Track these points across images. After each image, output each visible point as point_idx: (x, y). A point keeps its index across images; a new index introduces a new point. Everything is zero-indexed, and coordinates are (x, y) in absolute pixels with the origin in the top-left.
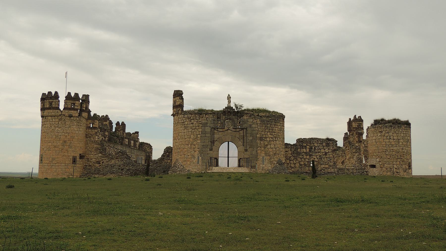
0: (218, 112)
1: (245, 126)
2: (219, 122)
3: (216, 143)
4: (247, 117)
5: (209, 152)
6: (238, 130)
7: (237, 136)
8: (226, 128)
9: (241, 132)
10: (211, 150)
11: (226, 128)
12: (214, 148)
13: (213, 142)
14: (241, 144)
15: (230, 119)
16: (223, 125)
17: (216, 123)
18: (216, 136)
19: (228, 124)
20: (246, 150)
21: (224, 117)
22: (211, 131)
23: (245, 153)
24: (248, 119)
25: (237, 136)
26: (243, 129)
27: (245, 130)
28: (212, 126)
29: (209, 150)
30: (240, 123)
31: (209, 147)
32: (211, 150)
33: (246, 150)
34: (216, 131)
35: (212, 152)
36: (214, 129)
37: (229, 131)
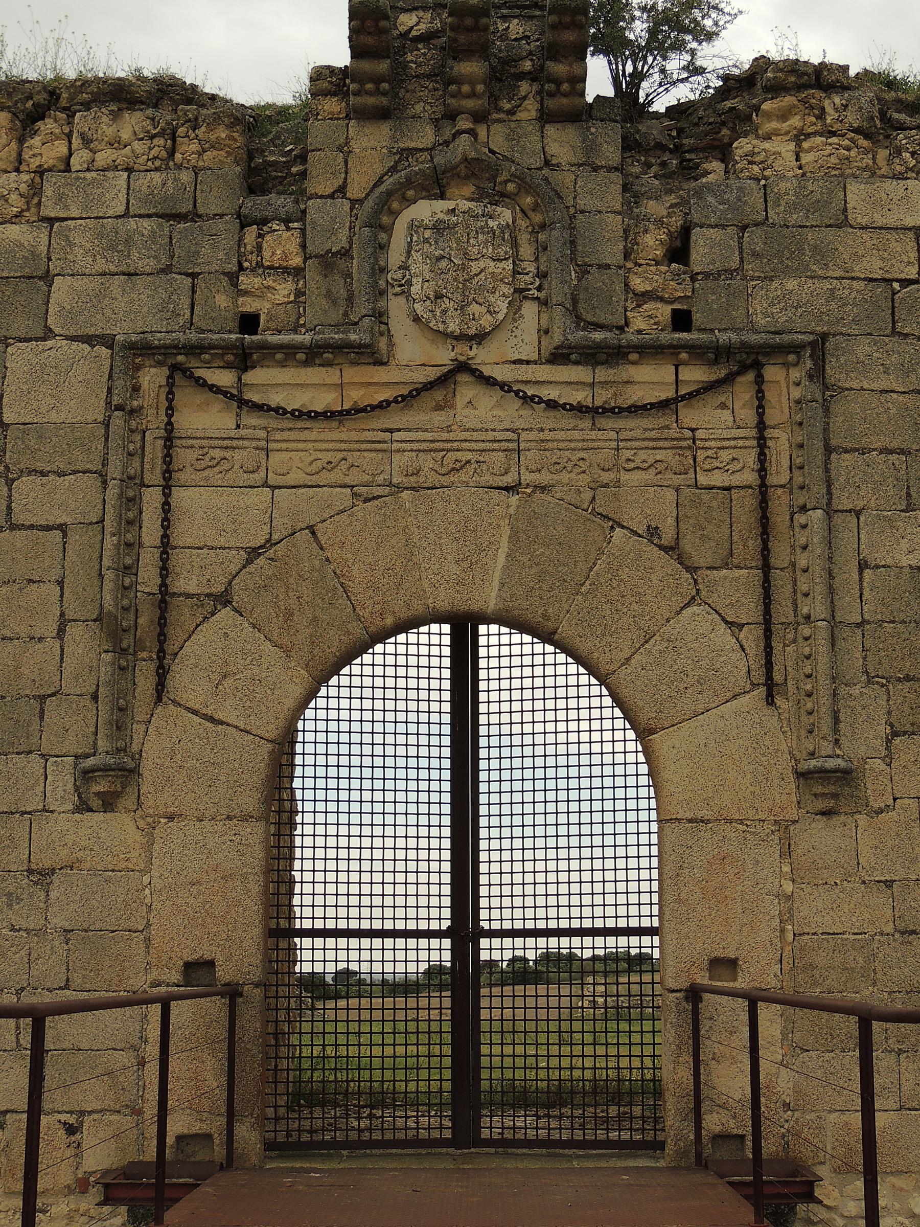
0: (254, 123)
1: (774, 305)
2: (282, 245)
3: (204, 648)
4: (819, 152)
5: (70, 833)
6: (651, 380)
7: (648, 499)
8: (414, 354)
9: (720, 421)
10: (109, 782)
11: (414, 354)
12: (162, 741)
13: (143, 634)
14: (734, 656)
15: (486, 179)
16: (356, 273)
17: (214, 251)
18: (214, 515)
19: (451, 270)
20: (830, 787)
21: (371, 145)
22: (122, 407)
23: (820, 838)
24: (840, 176)
25: (648, 499)
26: (744, 361)
27: (785, 384)
28: (135, 311)
29: (61, 783)
30: (678, 252)
31: (72, 727)
32: (109, 782)
33: (830, 787)
34: (203, 418)
35: (118, 830)
36: (180, 362)
37: (475, 408)
